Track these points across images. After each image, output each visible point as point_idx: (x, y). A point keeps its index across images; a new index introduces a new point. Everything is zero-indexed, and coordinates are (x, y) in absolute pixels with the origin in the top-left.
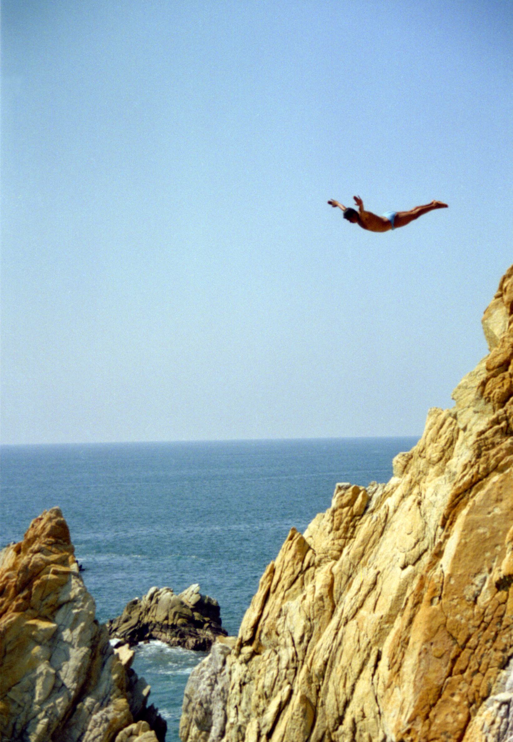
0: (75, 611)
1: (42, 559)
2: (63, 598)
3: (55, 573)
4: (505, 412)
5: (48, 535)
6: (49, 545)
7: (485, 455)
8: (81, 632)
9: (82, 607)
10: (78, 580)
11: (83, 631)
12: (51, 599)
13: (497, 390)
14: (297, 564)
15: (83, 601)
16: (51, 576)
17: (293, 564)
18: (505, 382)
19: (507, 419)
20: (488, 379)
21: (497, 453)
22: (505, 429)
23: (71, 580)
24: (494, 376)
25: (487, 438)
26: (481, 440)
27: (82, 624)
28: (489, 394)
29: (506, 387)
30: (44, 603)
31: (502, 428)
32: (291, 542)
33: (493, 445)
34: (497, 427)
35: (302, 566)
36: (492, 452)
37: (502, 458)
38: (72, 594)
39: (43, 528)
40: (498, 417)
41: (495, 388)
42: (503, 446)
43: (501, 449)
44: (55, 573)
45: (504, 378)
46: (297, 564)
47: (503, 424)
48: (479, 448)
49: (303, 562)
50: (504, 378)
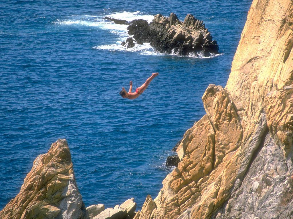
0: (70, 202)
1: (53, 171)
2: (63, 195)
3: (60, 180)
4: (177, 196)
5: (58, 157)
6: (58, 162)
7: (168, 214)
8: (72, 215)
9: (74, 200)
10: (73, 184)
11: (74, 214)
12: (58, 195)
13: (175, 186)
14: (148, 215)
15: (75, 197)
16: (58, 182)
17: (146, 215)
18: (179, 183)
19: (177, 200)
20: (172, 180)
21: (172, 214)
22: (176, 204)
23: (68, 184)
24: (175, 179)
25: (169, 207)
26: (167, 207)
27: (74, 210)
28: (172, 187)
29: (178, 185)
30: (53, 196)
31: (175, 203)
32: (146, 203)
33: (171, 210)
34: (173, 202)
35: (150, 217)
36: (170, 213)
37: (174, 216)
38: (68, 193)
39: (56, 152)
40: (174, 198)
41: (174, 185)
42: (174, 211)
43: (174, 212)
44: (60, 180)
45: (178, 181)
46: (148, 215)
47: (176, 201)
48: (166, 210)
49: (151, 215)
50: (178, 181)
